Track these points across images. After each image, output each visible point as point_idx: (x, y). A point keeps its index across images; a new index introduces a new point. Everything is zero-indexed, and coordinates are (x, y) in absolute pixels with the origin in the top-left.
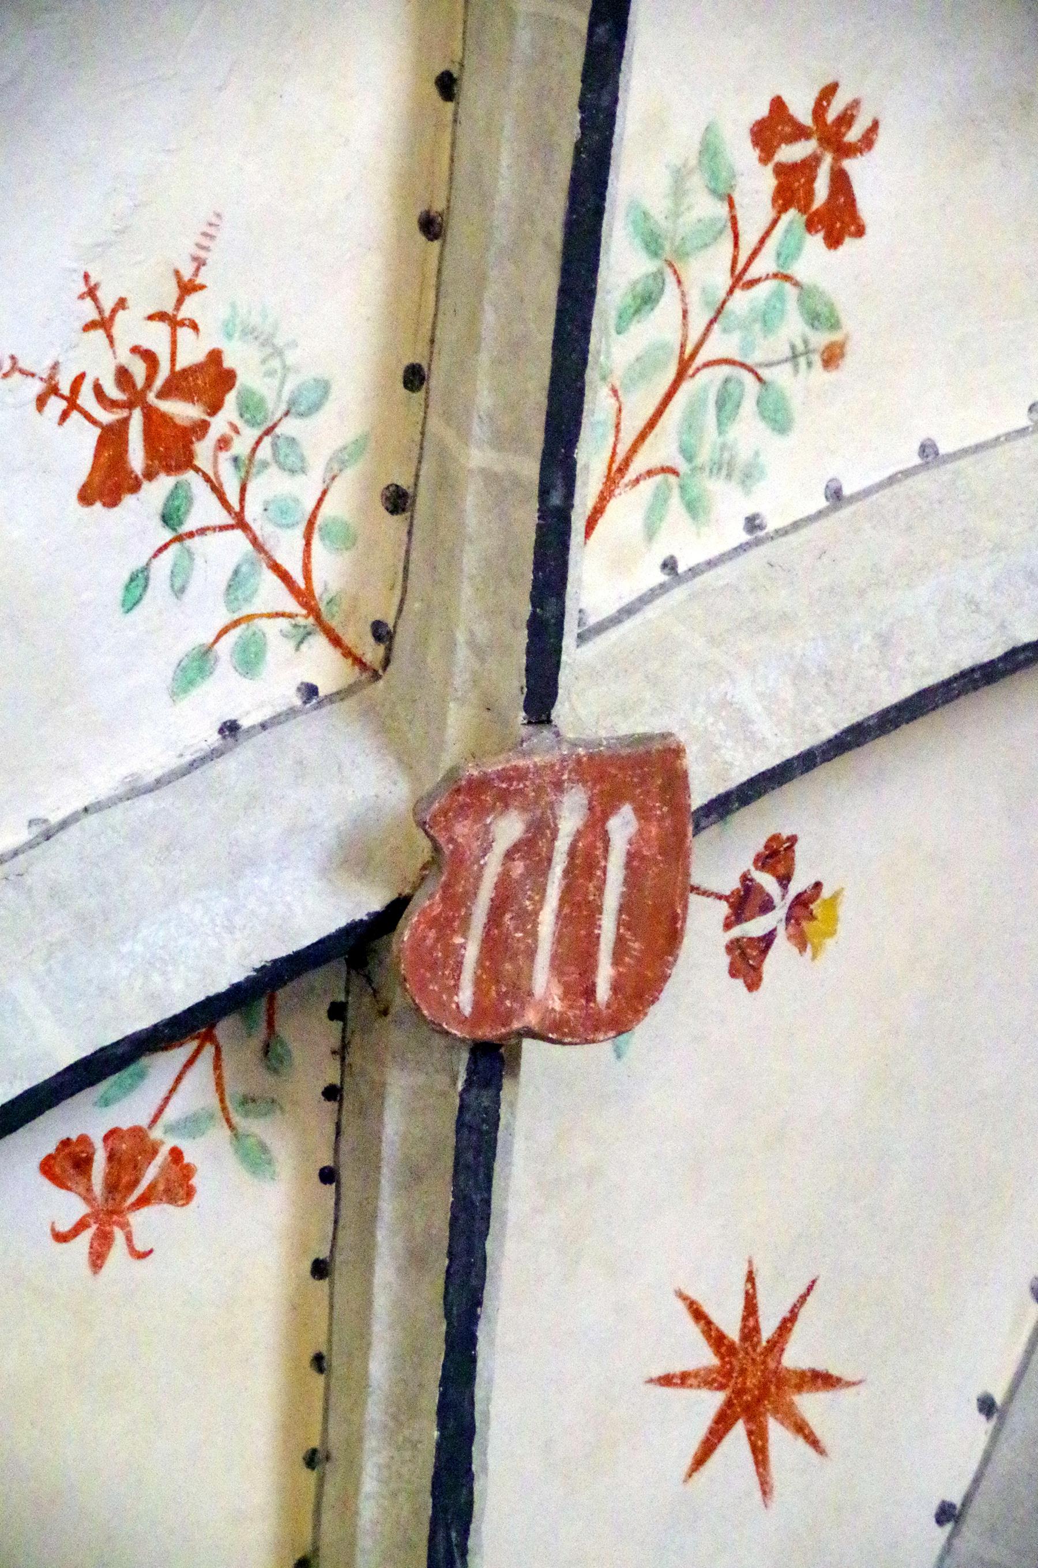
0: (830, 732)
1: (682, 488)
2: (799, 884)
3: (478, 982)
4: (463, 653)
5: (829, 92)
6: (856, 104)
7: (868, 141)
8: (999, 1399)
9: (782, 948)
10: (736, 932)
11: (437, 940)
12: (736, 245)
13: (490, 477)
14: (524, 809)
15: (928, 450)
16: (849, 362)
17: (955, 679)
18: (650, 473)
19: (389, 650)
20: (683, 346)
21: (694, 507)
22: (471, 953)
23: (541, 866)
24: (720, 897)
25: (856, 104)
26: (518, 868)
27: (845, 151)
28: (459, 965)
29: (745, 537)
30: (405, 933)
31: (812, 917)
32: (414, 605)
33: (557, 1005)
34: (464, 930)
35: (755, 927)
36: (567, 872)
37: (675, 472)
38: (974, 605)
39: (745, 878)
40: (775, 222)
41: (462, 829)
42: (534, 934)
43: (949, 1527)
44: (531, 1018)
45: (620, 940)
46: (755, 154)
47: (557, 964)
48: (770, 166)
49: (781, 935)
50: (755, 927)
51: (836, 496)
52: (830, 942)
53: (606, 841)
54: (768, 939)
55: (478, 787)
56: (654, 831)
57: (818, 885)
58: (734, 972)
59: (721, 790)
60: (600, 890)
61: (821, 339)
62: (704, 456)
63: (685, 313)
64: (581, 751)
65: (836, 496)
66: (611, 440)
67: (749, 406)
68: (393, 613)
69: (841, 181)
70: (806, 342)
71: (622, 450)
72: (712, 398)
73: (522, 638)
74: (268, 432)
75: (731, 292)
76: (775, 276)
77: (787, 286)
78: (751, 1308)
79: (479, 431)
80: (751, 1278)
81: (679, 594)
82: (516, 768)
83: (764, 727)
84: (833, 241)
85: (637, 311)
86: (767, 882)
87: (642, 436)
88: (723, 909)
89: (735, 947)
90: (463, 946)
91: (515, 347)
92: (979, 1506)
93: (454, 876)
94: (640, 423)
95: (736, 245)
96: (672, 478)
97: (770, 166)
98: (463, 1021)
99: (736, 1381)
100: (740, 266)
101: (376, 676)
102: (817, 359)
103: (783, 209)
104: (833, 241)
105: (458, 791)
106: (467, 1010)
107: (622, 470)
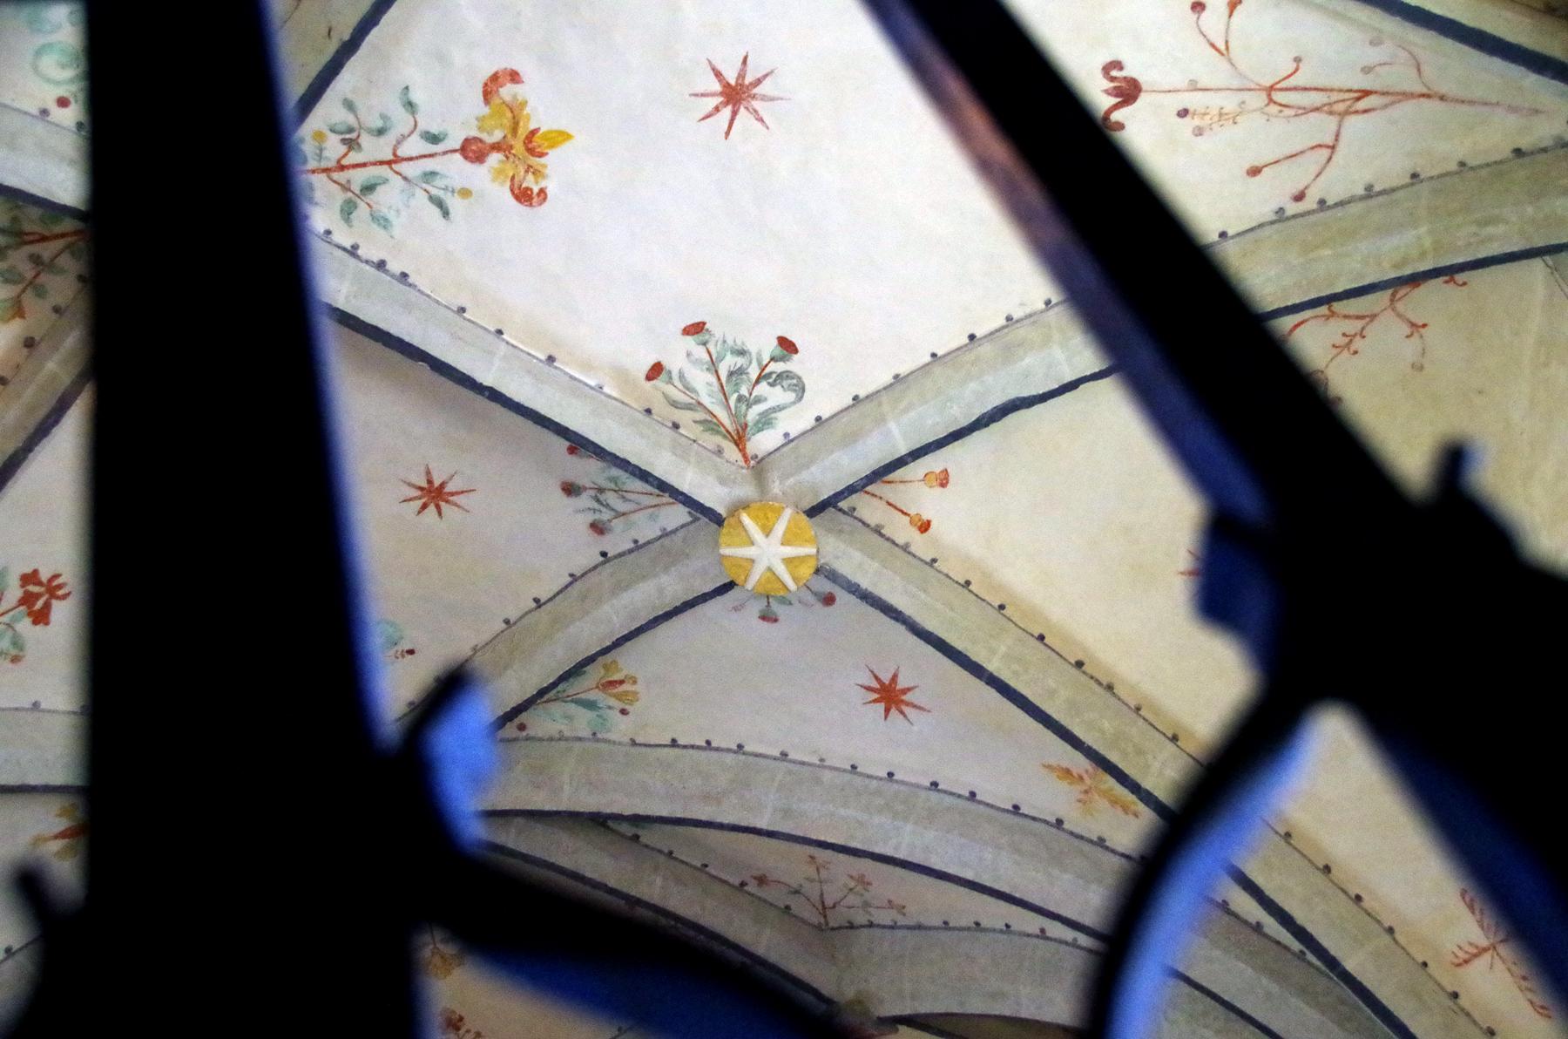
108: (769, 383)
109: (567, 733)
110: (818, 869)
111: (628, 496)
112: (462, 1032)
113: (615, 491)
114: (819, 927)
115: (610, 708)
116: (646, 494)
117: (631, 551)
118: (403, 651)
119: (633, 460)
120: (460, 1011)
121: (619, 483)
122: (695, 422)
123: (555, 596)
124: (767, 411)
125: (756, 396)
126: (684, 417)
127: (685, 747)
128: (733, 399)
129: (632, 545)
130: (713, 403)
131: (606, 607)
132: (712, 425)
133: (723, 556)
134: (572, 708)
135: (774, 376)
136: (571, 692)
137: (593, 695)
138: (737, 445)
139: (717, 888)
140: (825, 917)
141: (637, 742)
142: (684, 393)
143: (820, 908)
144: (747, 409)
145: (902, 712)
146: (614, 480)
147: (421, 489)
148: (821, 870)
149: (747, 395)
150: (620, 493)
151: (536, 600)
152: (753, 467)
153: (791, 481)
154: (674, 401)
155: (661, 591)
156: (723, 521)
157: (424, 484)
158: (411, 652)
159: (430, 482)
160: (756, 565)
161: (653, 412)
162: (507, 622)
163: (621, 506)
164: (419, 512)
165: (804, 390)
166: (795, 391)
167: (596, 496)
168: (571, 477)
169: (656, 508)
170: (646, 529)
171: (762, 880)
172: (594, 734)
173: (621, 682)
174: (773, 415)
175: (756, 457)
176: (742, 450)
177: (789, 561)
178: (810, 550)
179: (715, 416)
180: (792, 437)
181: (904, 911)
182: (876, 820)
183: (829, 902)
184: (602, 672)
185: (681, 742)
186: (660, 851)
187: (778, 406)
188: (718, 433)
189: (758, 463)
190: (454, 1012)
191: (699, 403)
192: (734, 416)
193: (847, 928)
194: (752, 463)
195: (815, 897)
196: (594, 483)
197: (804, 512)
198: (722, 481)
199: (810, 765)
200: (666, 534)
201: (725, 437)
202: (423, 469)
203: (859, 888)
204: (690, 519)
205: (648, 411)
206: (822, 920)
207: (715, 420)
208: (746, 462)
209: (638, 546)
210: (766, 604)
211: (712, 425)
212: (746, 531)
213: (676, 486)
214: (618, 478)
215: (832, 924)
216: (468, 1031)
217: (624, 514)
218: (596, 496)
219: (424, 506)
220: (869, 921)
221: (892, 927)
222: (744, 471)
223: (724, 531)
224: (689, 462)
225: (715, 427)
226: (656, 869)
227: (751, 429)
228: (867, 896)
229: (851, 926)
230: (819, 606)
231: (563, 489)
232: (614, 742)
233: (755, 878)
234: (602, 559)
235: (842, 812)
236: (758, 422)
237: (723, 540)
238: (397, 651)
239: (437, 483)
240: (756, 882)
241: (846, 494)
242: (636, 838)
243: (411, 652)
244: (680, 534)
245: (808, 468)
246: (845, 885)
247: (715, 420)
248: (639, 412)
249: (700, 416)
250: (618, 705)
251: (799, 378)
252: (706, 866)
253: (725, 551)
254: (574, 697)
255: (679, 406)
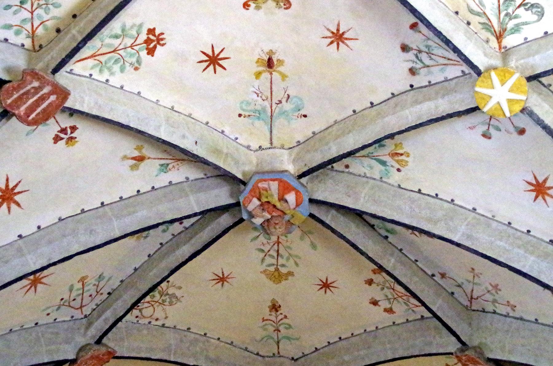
0: (94, 113)
1: (101, 66)
2: (73, 135)
3: (13, 101)
4: (49, 57)
5: (163, 34)
6: (165, 39)
7: (163, 45)
8: (41, 228)
9: (63, 142)
10: (59, 134)
11: (12, 90)
12: (135, 42)
13: (74, 36)
14: (41, 83)
15: (139, 93)
16: (138, 72)
17: (117, 122)
18: (98, 60)
19: (40, 50)
20: (117, 48)
21: (101, 71)
22: (15, 96)
23: (36, 93)
24: (60, 127)
25: (165, 39)
26: (32, 91)
27: (158, 43)
28: (11, 97)
29: (105, 81)
30: (7, 85)
31: (71, 141)
32: (49, 46)
33: (22, 114)
34: (17, 92)
35: (62, 135)
36: (39, 97)
37: (102, 63)
38: (128, 116)
39: (66, 128)
40: (142, 44)
41: (28, 78)
42: (27, 101)
43: (19, 238)
44: (16, 112)
45: (39, 113)
46: (146, 32)
47: (27, 109)
48: (147, 36)
49: (65, 139)
50: (62, 135)
51: (122, 87)
52: (71, 147)
53: (49, 98)
54: (62, 139)
55: (37, 74)
56: (57, 102)
57: (76, 138)
58: (54, 139)
59: (72, 107)
60: (42, 104)
61: (136, 65)
62: (108, 65)
63: (120, 44)
64: (55, 82)
65: (122, 87)
66: (97, 51)
67: (119, 65)
68: (45, 45)
69: (155, 47)
70: (134, 63)
71: (97, 53)
72: (115, 58)
73: (59, 60)
74: (47, 4)
75: (129, 47)
76: (137, 51)
77: (137, 54)
78: (16, 186)
79: (77, 28)
80: (20, 182)
81: (88, 79)
82: (44, 76)
83: (85, 105)
84: (148, 54)
85: (114, 37)
86: (69, 131)
87: (101, 54)
88: (59, 129)
89: (57, 136)
90: (15, 94)
91: (91, 21)
92: (25, 239)
93: (22, 83)
94: (102, 53)
95: (135, 42)
96: (101, 64)
97: (147, 36)
98: (5, 104)
99: (4, 194)
100: (133, 45)
101: (35, 52)
102: (134, 67)
103: (144, 43)
104: (148, 54)
105: (32, 72)
106: (8, 103)
107: (95, 56)
108: (525, 9)
109: (368, 175)
110: (474, 277)
111: (433, 56)
112: (278, 313)
113: (427, 53)
114: (466, 307)
115: (392, 166)
116: (443, 57)
117: (426, 87)
118: (301, 115)
119: (444, 33)
120: (280, 302)
121: (431, 49)
122: (480, 23)
123: (381, 103)
124: (519, 24)
125: (516, 15)
126: (475, 20)
127: (424, 194)
128: (502, 15)
129: (427, 84)
130: (492, 14)
131: (407, 111)
132: (487, 26)
133: (477, 92)
134: (374, 163)
135: (529, 5)
136: (375, 154)
137: (387, 159)
138: (498, 39)
139: (421, 273)
140: (471, 303)
141: (401, 187)
142: (478, 6)
143: (470, 297)
144: (509, 21)
145: (544, 200)
146: (428, 47)
147: (333, 33)
148: (476, 277)
149: (511, 13)
150: (429, 54)
151: (372, 103)
152: (503, 53)
153: (522, 61)
154: (472, 10)
155: (437, 107)
156: (481, 74)
157: (335, 31)
158: (305, 116)
159: (338, 30)
160: (492, 99)
161: (459, 14)
162: (354, 111)
163: (427, 62)
164: (329, 45)
165: (543, 15)
166: (538, 15)
167: (417, 54)
168: (407, 42)
169: (445, 66)
170: (437, 76)
171: (443, 276)
172: (381, 178)
173: (402, 155)
174: (523, 27)
175: (506, 47)
176: (499, 43)
177: (510, 101)
178: (524, 98)
179: (490, 22)
180: (528, 40)
181: (515, 308)
182: (516, 250)
183: (475, 296)
184: (393, 147)
185: (423, 191)
186: (397, 248)
187: (526, 22)
188: (490, 31)
189: (506, 51)
190: (277, 302)
191: (485, 13)
192: (501, 23)
193: (481, 311)
194: (503, 50)
195: (468, 291)
196: (417, 47)
197: (526, 78)
198: (486, 55)
199: (486, 217)
200: (446, 80)
201: (492, 34)
202: (336, 23)
203: (493, 292)
204: (462, 74)
205: (457, 13)
206: (469, 305)
207: (490, 24)
208: (499, 49)
209: (430, 84)
210: (487, 128)
211: (487, 26)
212: (492, 81)
213: (463, 51)
214: (431, 46)
215: (473, 308)
216: (281, 314)
217: (428, 66)
218: (417, 54)
219: (332, 43)
220: (494, 310)
221: (505, 316)
222: (498, 54)
223: (480, 79)
224: (471, 41)
225: (489, 28)
226: (392, 255)
227: (508, 32)
228: (497, 297)
229: (484, 311)
230: (515, 135)
231: (401, 48)
232: (390, 184)
233: (440, 274)
234: (410, 88)
235: (498, 243)
236: (513, 29)
237: (478, 83)
238: (299, 114)
239: (341, 32)
240: (439, 276)
241: (550, 73)
242: (386, 237)
243: (305, 116)
244: (454, 81)
245: (534, 56)
246: (486, 288)
247: (490, 24)
248: (452, 12)
249: (483, 20)
250: (397, 166)
251: (543, 9)
252: (417, 261)
253: (477, 89)
254: (376, 157)
255: (473, 12)
